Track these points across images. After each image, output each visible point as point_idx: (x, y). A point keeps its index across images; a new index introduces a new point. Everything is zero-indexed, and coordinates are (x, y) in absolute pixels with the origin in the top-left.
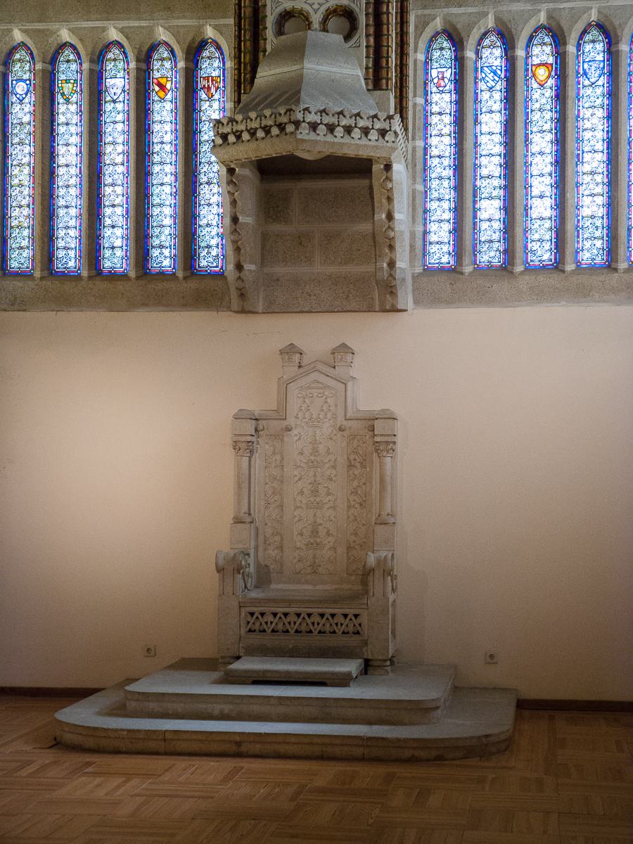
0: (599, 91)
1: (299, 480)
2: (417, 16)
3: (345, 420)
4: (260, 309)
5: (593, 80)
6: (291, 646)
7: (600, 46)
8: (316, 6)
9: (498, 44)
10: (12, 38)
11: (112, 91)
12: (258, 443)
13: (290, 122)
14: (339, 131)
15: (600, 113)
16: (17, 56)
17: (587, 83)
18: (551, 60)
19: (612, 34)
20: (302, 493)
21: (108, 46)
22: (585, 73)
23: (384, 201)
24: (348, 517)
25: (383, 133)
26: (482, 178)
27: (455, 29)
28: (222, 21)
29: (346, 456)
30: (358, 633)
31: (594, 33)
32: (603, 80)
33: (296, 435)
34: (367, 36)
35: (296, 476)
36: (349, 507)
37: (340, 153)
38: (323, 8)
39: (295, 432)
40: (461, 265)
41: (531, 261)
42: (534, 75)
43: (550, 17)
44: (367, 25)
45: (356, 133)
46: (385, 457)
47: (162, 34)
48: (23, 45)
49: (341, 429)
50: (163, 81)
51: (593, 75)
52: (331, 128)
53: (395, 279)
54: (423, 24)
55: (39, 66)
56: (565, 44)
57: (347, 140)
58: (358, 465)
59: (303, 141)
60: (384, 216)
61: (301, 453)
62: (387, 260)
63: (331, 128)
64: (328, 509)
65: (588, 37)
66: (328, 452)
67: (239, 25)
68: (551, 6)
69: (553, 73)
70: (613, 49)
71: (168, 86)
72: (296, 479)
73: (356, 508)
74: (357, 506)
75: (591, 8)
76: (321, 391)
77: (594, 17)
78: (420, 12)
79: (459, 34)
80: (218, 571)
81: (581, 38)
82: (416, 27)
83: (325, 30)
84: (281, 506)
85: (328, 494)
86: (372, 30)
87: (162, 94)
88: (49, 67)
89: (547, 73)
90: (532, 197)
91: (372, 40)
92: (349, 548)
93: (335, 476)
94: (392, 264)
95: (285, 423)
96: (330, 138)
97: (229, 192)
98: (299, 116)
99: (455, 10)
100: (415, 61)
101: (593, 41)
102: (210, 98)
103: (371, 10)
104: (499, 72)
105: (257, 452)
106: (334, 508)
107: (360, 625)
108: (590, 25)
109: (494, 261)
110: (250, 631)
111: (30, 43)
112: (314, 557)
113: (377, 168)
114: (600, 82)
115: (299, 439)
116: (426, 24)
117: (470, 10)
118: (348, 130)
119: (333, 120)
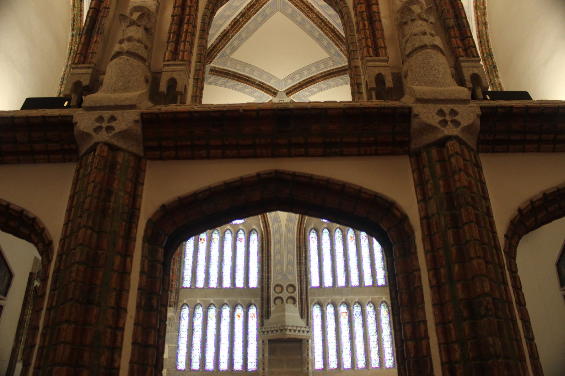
2: (310, 299)
7: (359, 308)
8: (285, 296)
10: (197, 302)
11: (224, 317)
13: (284, 329)
14: (297, 331)
16: (197, 307)
18: (346, 311)
19: (362, 306)
21: (224, 304)
22: (356, 315)
23: (306, 350)
25: (308, 332)
27: (320, 302)
28: (256, 299)
31: (357, 304)
32: (361, 317)
34: (299, 304)
37: (296, 337)
38: (287, 297)
40: (326, 368)
43: (345, 300)
44: (299, 302)
45: (301, 332)
47: (239, 302)
48: (199, 304)
50: (239, 315)
51: (358, 315)
52: (295, 331)
53: (309, 373)
54: (312, 301)
55: (204, 310)
56: (350, 307)
57: (299, 334)
59: (288, 334)
60: (306, 355)
62: (306, 367)
63: (295, 331)
65: (355, 305)
67: (262, 300)
68: (346, 297)
70: (363, 308)
71: (240, 316)
75: (356, 298)
78: (311, 298)
79: (322, 304)
81: (354, 306)
82: (310, 302)
83: (287, 303)
86: (300, 303)
87: (239, 318)
88: (206, 310)
91: (300, 305)
94: (308, 368)
96: (294, 333)
97: (262, 348)
98: (286, 328)
99: (320, 297)
100: (310, 311)
101: (357, 306)
102: (253, 319)
103: (300, 297)
108: (356, 302)
111: (202, 303)
113: (303, 341)
116: (313, 301)
117: (325, 297)
118: (299, 331)
119: (295, 328)
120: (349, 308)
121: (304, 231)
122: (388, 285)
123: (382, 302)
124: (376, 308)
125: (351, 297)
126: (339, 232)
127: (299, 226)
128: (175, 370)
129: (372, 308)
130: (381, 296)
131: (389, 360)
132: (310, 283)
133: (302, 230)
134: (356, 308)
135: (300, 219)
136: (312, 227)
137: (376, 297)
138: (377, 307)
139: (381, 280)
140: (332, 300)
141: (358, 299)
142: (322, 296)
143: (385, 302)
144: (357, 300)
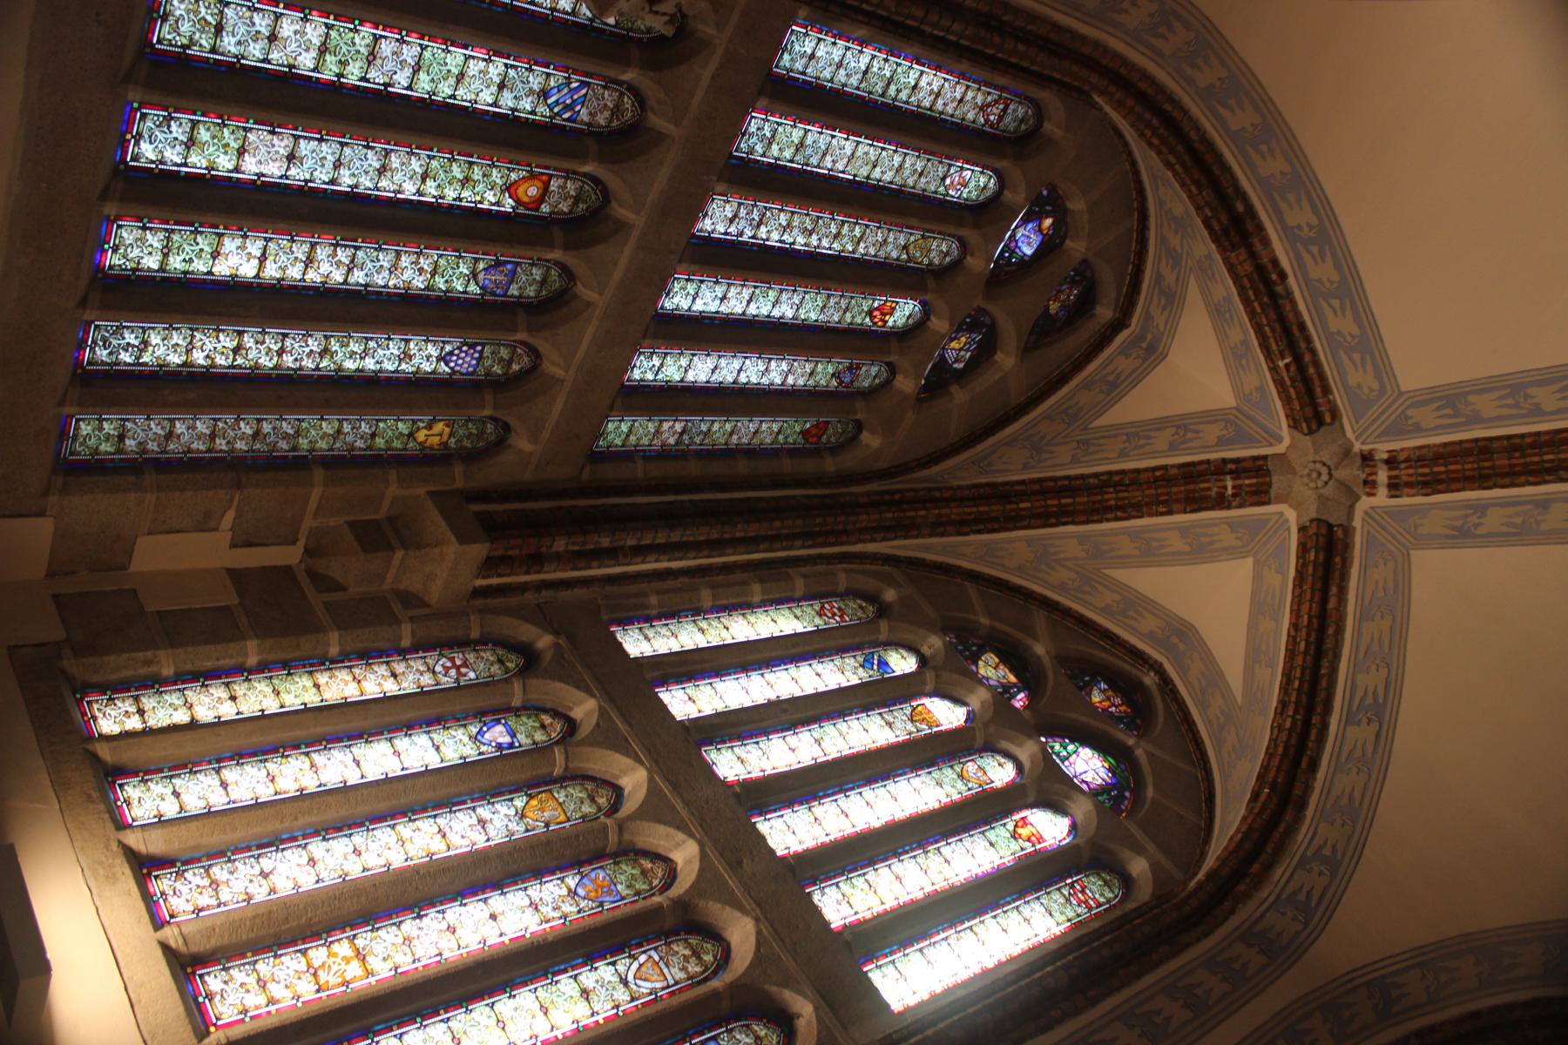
0: (459, 286)
5: (481, 276)
7: (531, 291)
9: (615, 123)
15: (419, 283)
17: (481, 266)
18: (545, 208)
26: (376, 38)
41: (144, 116)
42: (532, 176)
56: (567, 247)
68: (636, 233)
69: (521, 210)
75: (601, 294)
77: (583, 291)
89: (526, 199)
90: (296, 138)
99: (712, 67)
101: (543, 282)
104: (566, 116)
109: (166, 28)
114: (473, 288)
117: (699, 94)
120: (558, 234)
121: (1078, 90)
122: (586, 476)
123: (507, 428)
124: (489, 397)
125: (623, 262)
126: (947, 254)
127: (1142, 85)
129: (497, 369)
130: (546, 435)
131: (121, 437)
132: (814, 23)
133: (1095, 78)
134: (537, 273)
135: (1168, 107)
136: (1047, 125)
137: (558, 406)
138: (495, 407)
139: (619, 430)
140: (659, 138)
141: (589, 305)
142: (713, 78)
143: (500, 444)
144: (580, 288)
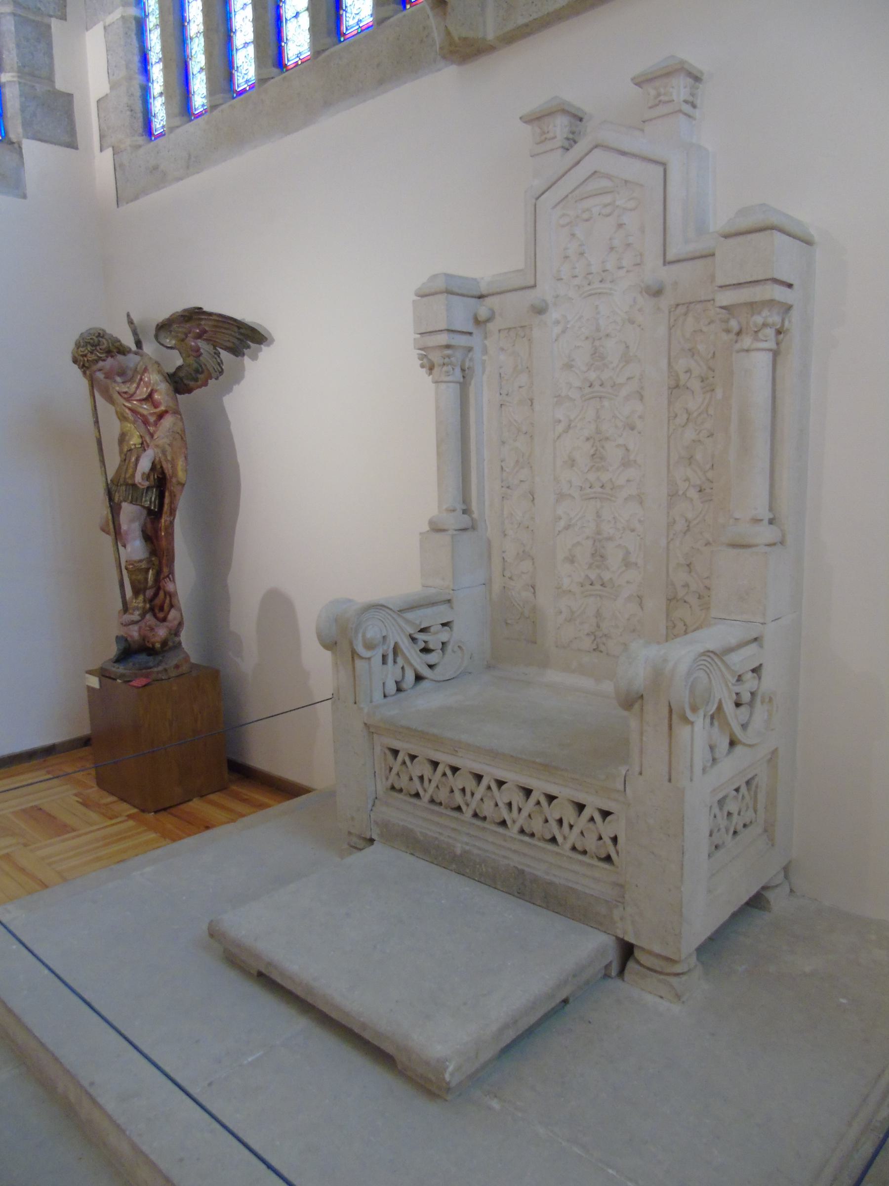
1: (566, 431)
3: (665, 263)
4: (490, 32)
6: (458, 851)
12: (485, 351)
20: (572, 463)
24: (671, 524)
29: (664, 364)
30: (608, 859)
33: (557, 322)
35: (560, 421)
36: (673, 495)
39: (554, 314)
46: (747, 351)
49: (657, 292)
58: (696, 384)
61: (569, 366)
64: (626, 499)
66: (627, 359)
72: (560, 428)
73: (691, 500)
74: (693, 493)
76: (607, 199)
80: (327, 647)
84: (532, 496)
85: (626, 464)
92: (672, 600)
93: (640, 417)
95: (531, 296)
105: (483, 372)
106: (640, 499)
107: (615, 840)
110: (393, 788)
112: (598, 614)
115: (564, 332)
128: (141, 140)
